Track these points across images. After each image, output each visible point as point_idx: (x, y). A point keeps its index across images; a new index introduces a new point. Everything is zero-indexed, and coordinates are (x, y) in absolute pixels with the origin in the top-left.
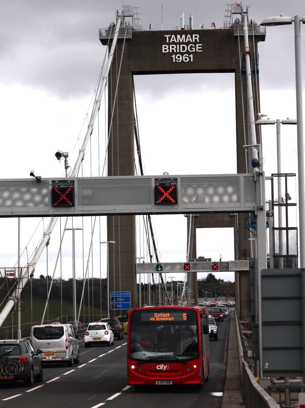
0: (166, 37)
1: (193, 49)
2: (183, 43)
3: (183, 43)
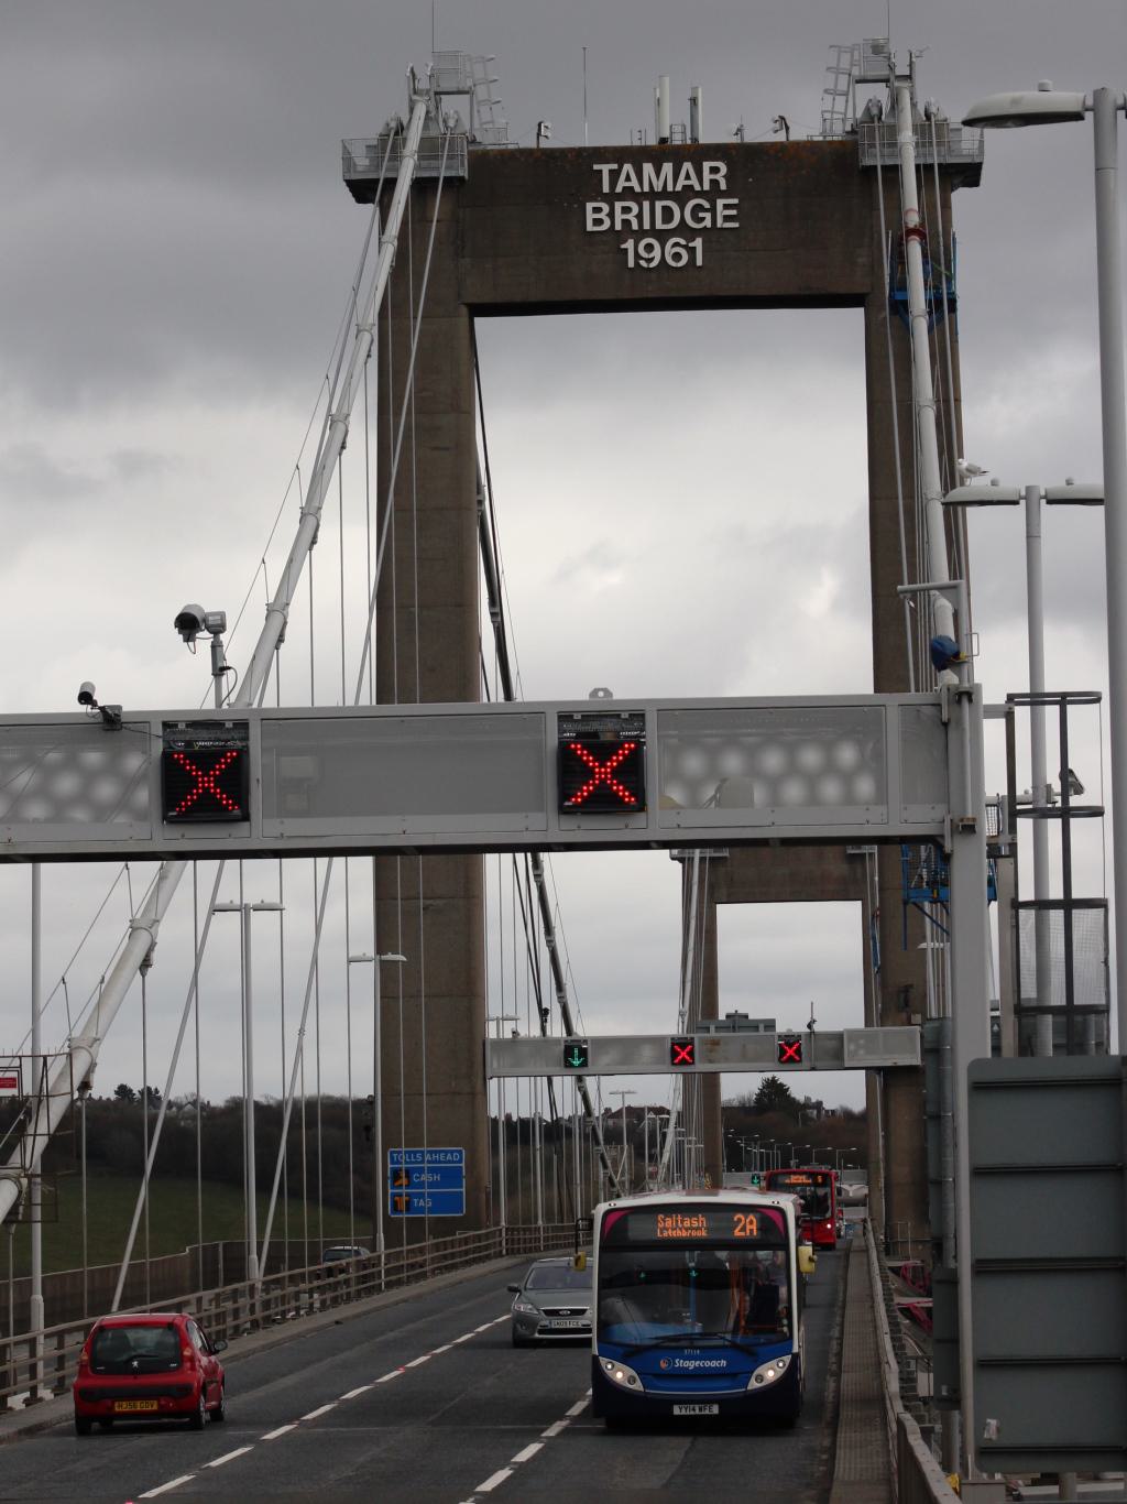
0: (601, 171)
1: (703, 219)
2: (664, 195)
3: (664, 195)
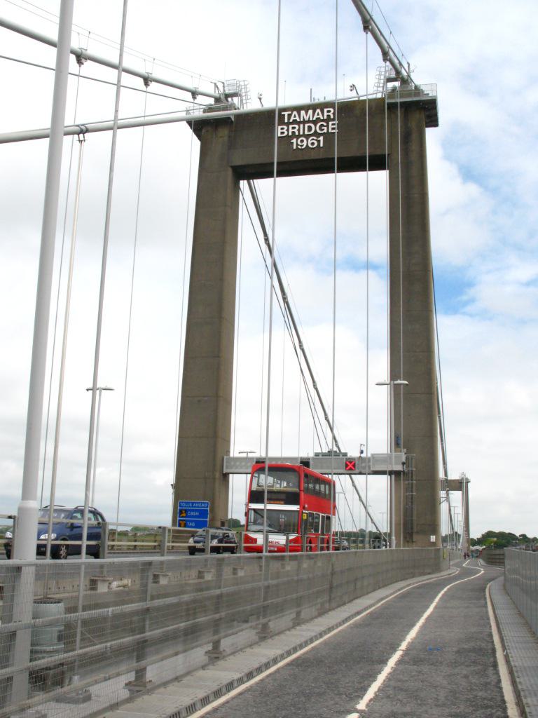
1: (323, 130)
2: (309, 121)
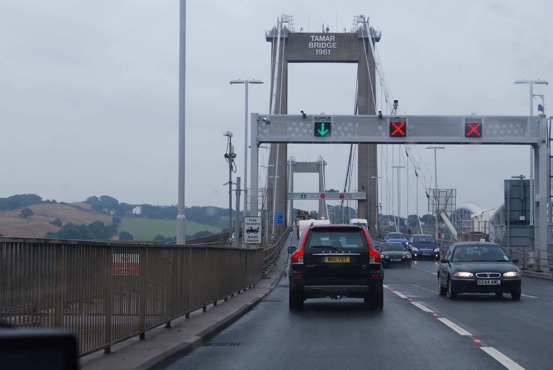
2: (323, 42)
3: (323, 42)
